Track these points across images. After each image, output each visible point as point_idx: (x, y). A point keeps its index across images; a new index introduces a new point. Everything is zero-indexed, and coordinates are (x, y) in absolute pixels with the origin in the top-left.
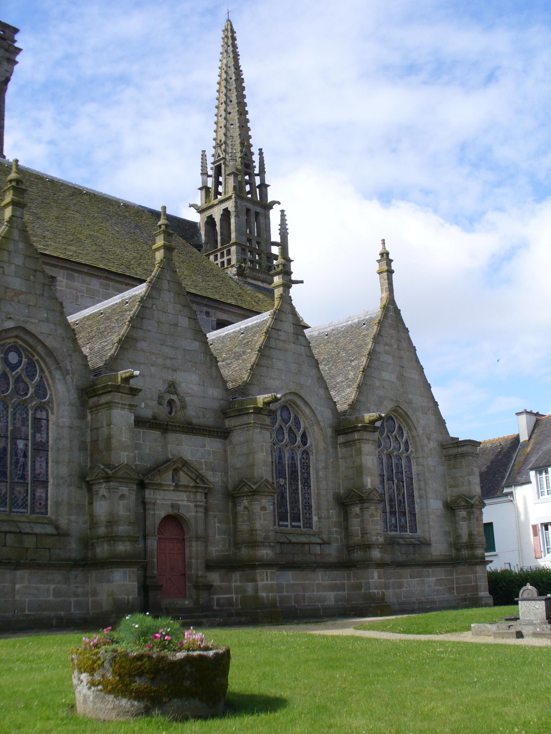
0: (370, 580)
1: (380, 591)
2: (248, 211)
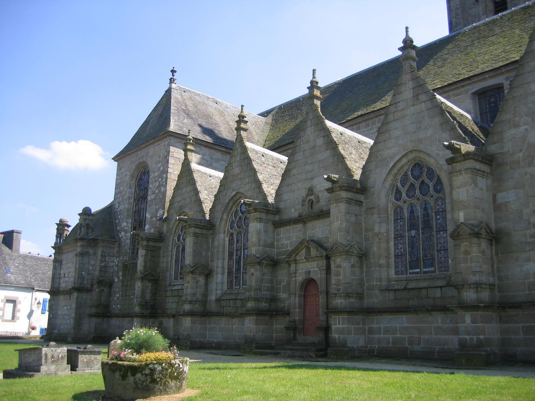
0: (459, 325)
1: (475, 338)
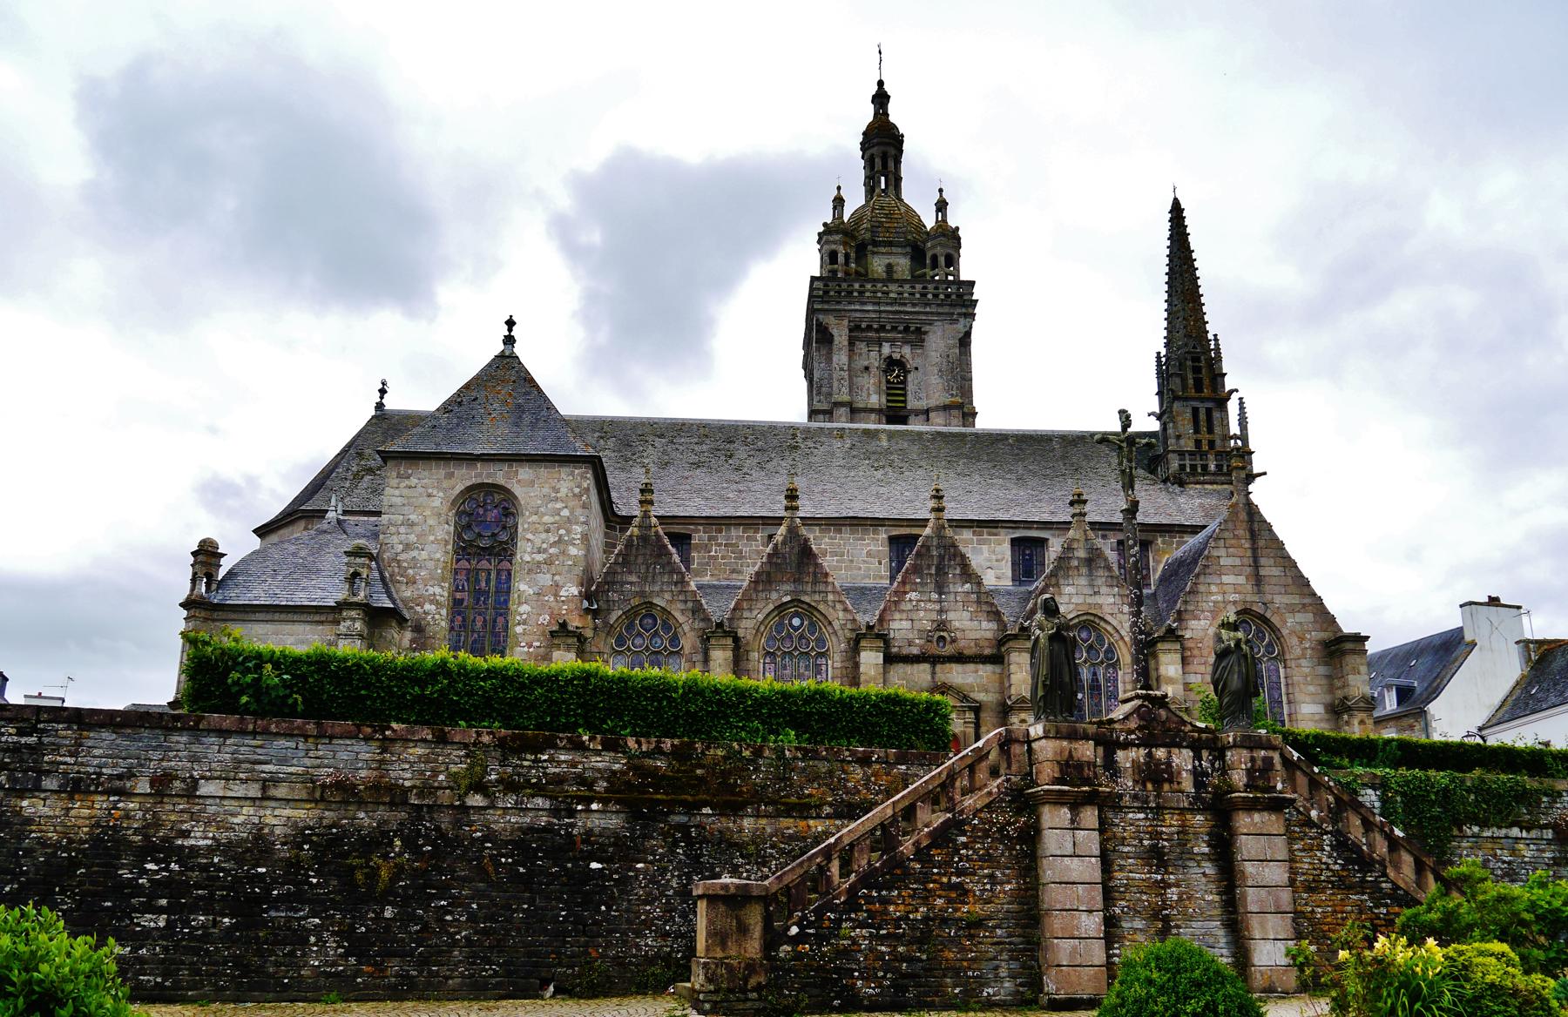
2: (1195, 411)
